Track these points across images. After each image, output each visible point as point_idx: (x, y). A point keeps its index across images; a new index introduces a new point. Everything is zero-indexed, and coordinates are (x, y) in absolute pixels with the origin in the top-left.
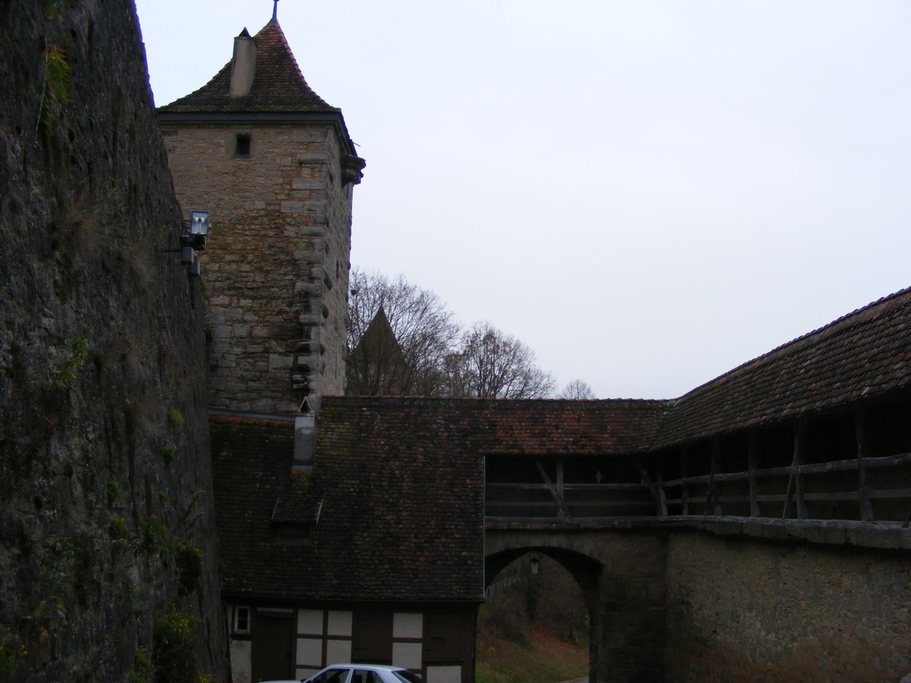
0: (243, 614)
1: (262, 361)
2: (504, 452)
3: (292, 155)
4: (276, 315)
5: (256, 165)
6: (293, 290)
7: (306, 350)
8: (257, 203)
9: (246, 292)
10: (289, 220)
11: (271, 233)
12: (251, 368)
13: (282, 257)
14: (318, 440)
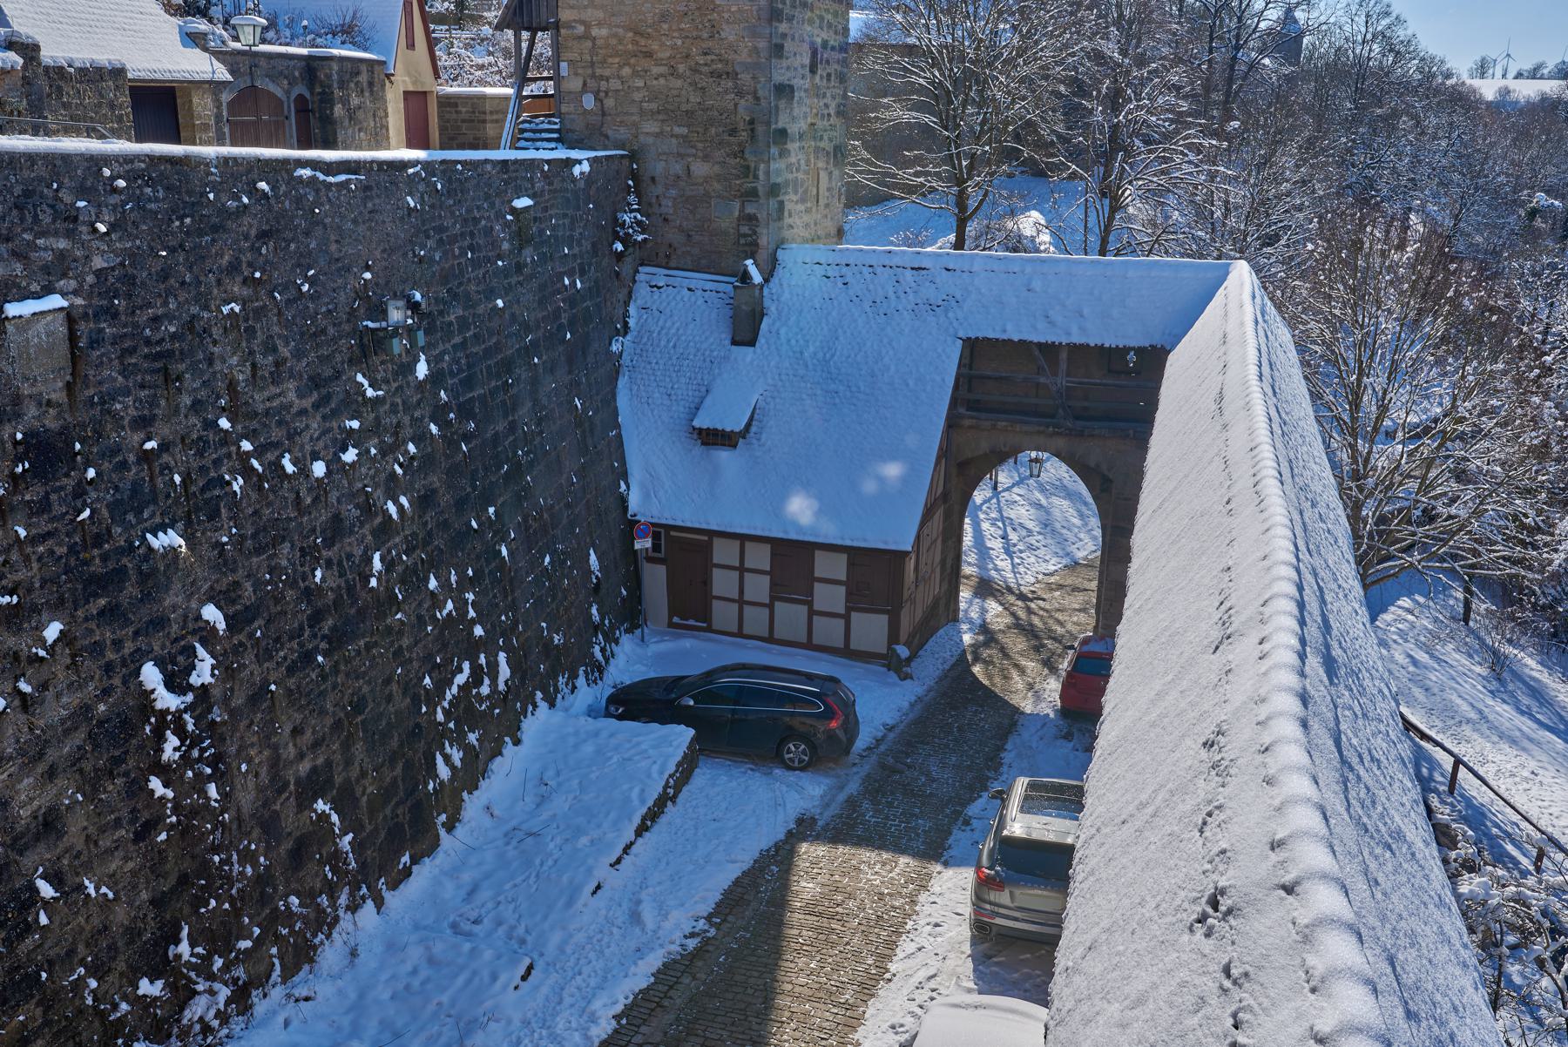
7: (753, 194)
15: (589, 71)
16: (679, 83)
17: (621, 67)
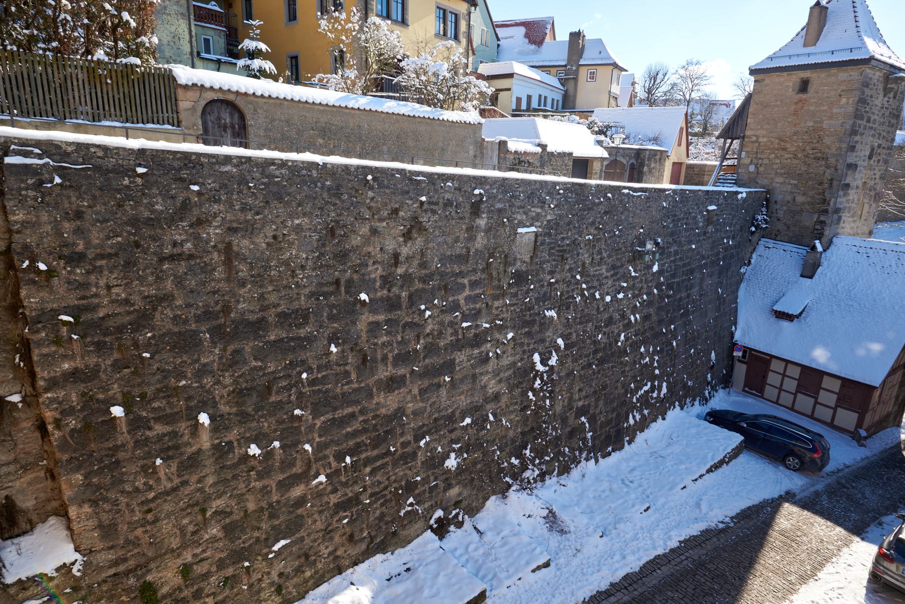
7: (826, 212)
15: (755, 156)
16: (797, 162)
17: (770, 154)
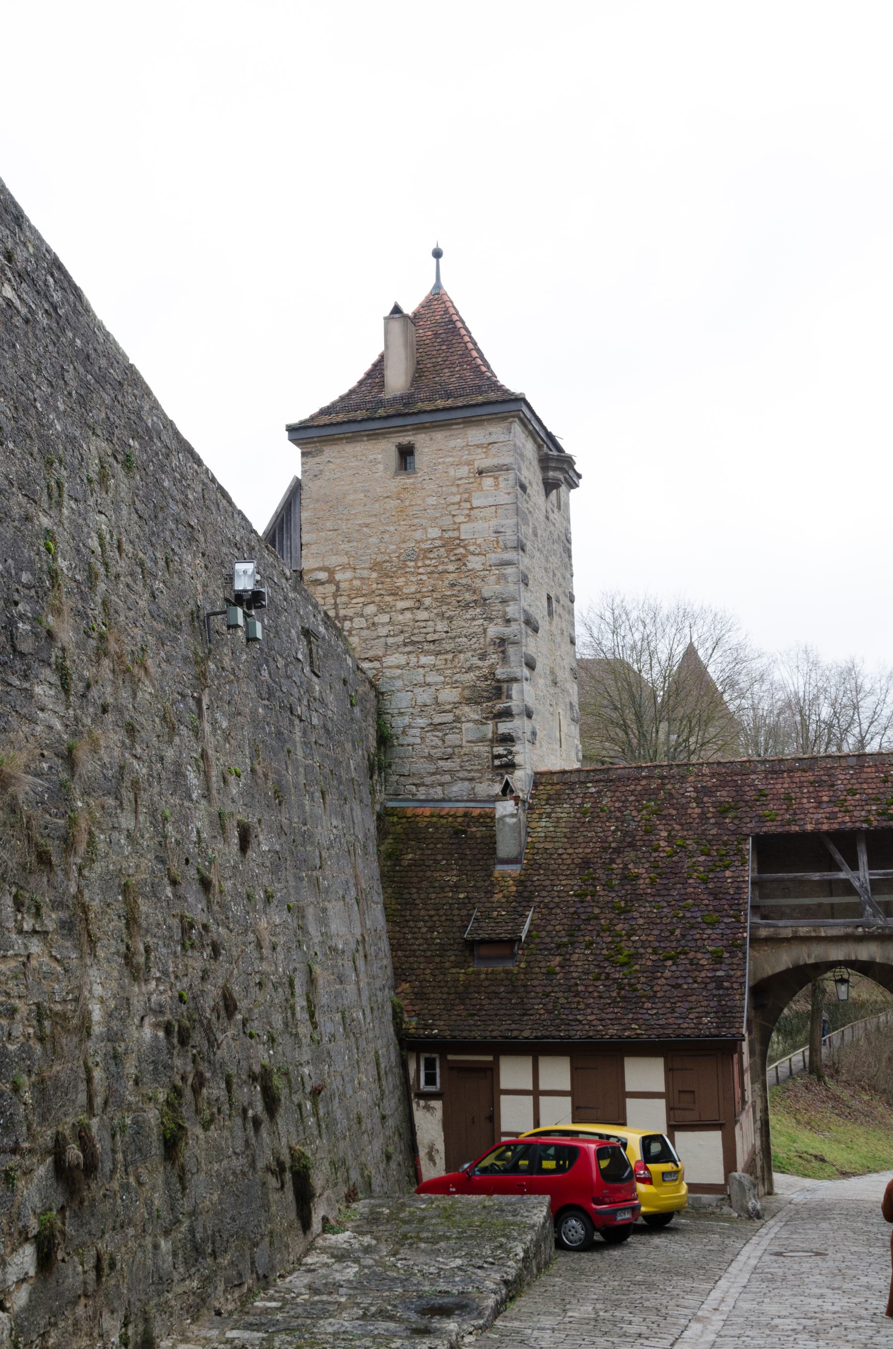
0: (430, 1065)
1: (453, 733)
2: (780, 830)
3: (469, 463)
4: (466, 672)
5: (424, 482)
6: (485, 637)
7: (507, 714)
8: (430, 530)
9: (426, 647)
10: (472, 548)
11: (451, 568)
12: (440, 743)
13: (468, 596)
14: (529, 830)
